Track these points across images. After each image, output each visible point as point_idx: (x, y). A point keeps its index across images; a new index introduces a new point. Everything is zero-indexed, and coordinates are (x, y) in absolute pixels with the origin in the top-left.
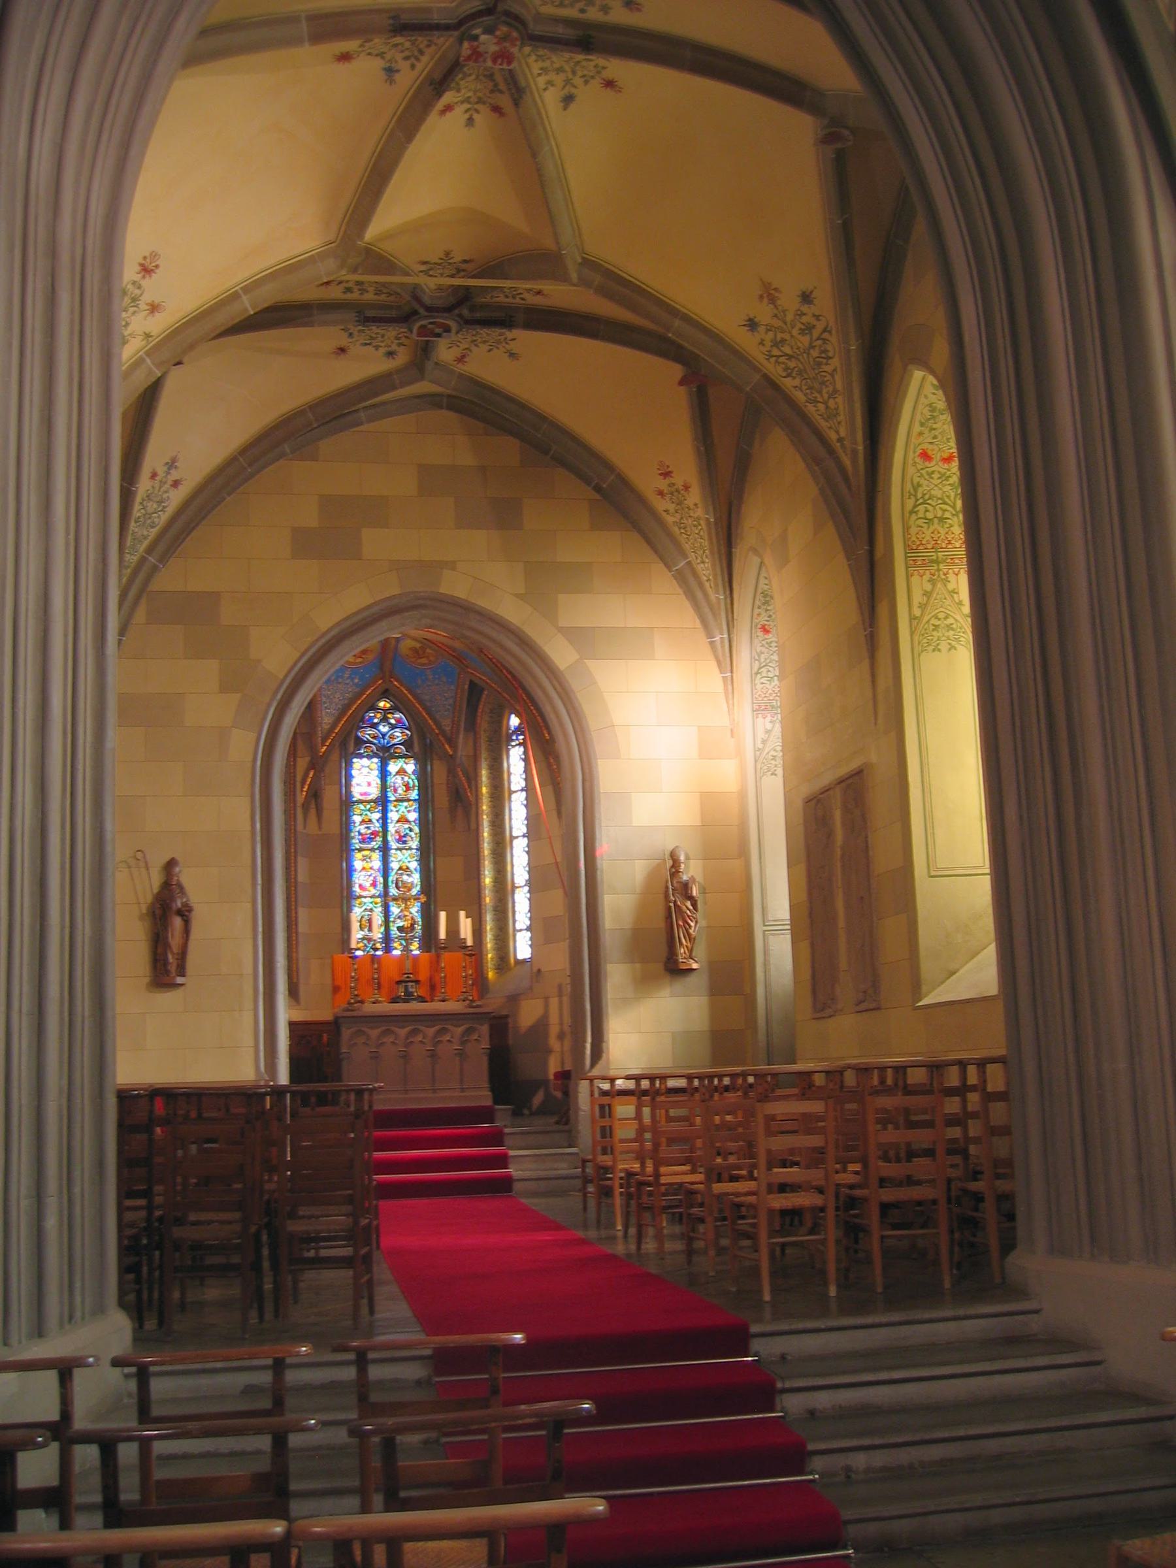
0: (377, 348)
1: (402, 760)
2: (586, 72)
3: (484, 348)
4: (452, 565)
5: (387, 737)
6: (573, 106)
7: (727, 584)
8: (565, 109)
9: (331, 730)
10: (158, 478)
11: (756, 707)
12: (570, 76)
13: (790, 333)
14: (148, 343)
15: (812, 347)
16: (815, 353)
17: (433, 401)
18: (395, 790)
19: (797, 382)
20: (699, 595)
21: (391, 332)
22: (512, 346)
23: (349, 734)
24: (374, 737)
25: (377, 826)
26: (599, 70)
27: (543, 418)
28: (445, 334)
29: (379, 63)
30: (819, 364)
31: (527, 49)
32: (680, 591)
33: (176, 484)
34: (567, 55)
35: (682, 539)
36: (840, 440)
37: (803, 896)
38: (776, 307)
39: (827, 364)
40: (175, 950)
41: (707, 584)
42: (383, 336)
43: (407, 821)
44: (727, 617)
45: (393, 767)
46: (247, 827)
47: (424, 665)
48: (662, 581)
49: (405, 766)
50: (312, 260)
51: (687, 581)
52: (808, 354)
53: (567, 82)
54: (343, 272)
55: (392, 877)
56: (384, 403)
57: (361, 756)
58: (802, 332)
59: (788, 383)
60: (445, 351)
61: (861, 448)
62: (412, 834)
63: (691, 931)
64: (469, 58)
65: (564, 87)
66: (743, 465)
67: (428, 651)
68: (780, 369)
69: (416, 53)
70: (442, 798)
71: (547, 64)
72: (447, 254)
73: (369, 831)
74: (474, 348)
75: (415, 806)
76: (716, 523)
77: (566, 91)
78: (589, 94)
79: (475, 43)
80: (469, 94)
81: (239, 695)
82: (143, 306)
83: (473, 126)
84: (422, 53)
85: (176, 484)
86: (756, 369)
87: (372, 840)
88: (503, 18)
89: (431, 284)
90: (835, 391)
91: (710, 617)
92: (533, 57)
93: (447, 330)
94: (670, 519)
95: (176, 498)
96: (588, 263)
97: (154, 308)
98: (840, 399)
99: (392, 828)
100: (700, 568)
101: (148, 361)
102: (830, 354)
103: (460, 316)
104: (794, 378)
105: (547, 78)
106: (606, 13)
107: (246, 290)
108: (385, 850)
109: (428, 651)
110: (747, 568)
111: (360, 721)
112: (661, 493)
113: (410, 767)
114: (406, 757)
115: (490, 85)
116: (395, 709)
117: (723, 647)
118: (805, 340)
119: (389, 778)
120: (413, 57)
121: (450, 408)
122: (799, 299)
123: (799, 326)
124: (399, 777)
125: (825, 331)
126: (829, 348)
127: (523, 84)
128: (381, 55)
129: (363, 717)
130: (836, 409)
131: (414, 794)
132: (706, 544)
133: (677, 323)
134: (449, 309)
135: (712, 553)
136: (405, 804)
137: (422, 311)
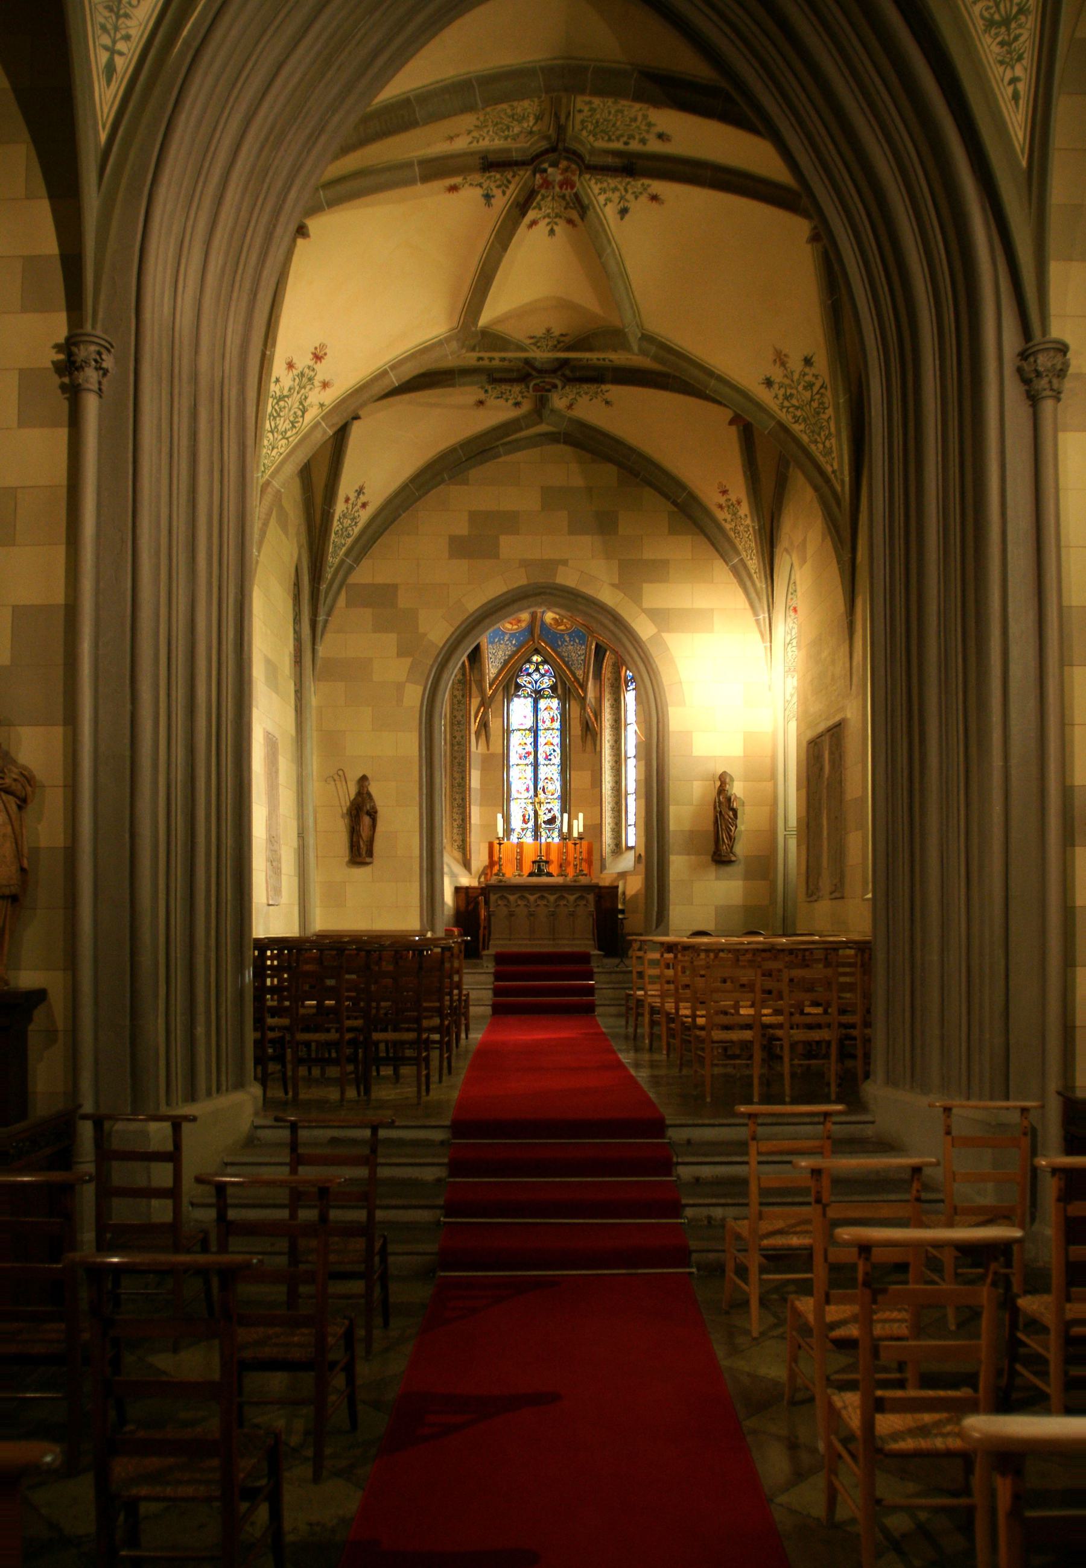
0: (507, 400)
1: (549, 700)
2: (635, 190)
3: (586, 398)
4: (565, 562)
5: (538, 684)
6: (627, 217)
7: (769, 577)
8: (622, 219)
9: (496, 678)
10: (350, 502)
11: (787, 668)
12: (624, 193)
13: (797, 389)
14: (322, 411)
15: (812, 400)
16: (815, 405)
17: (553, 438)
18: (544, 722)
19: (802, 427)
20: (749, 584)
21: (516, 389)
22: (607, 396)
23: (510, 680)
24: (529, 683)
25: (530, 748)
26: (645, 188)
27: (632, 449)
28: (553, 390)
29: (478, 192)
30: (818, 413)
31: (588, 176)
32: (735, 581)
33: (364, 505)
34: (619, 179)
35: (737, 541)
36: (834, 472)
37: (804, 814)
38: (786, 369)
39: (824, 413)
40: (365, 838)
41: (755, 576)
42: (510, 391)
43: (552, 744)
44: (768, 601)
45: (543, 703)
46: (417, 754)
47: (562, 630)
48: (721, 572)
49: (551, 705)
50: (440, 343)
51: (740, 573)
52: (810, 406)
53: (622, 198)
54: (464, 351)
55: (540, 785)
56: (516, 441)
57: (519, 696)
58: (805, 388)
59: (797, 428)
60: (558, 401)
61: (847, 479)
62: (555, 753)
63: (732, 834)
64: (541, 186)
65: (620, 202)
66: (781, 484)
67: (565, 620)
68: (790, 417)
69: (505, 182)
70: (576, 729)
71: (605, 185)
72: (548, 330)
73: (525, 751)
74: (578, 398)
75: (558, 733)
76: (760, 530)
77: (621, 205)
78: (640, 207)
79: (545, 175)
80: (548, 211)
81: (410, 660)
82: (316, 383)
83: (554, 235)
84: (509, 182)
85: (364, 505)
86: (772, 417)
87: (526, 758)
88: (564, 154)
89: (541, 355)
90: (830, 434)
91: (756, 601)
92: (593, 181)
93: (555, 386)
94: (727, 526)
95: (364, 516)
96: (647, 338)
97: (325, 385)
98: (833, 441)
99: (541, 750)
100: (749, 563)
101: (323, 424)
102: (826, 405)
103: (563, 375)
104: (800, 424)
105: (606, 195)
106: (645, 144)
107: (393, 367)
108: (536, 765)
109: (565, 620)
110: (783, 562)
111: (519, 671)
112: (721, 507)
113: (555, 703)
114: (552, 697)
115: (564, 203)
116: (545, 662)
117: (765, 623)
118: (807, 395)
119: (539, 713)
120: (504, 186)
121: (565, 443)
122: (803, 363)
123: (803, 383)
124: (546, 712)
125: (822, 387)
126: (826, 400)
127: (586, 202)
128: (480, 185)
129: (521, 668)
130: (831, 448)
131: (557, 725)
132: (753, 545)
133: (713, 382)
134: (554, 371)
135: (757, 552)
136: (551, 731)
137: (534, 373)
